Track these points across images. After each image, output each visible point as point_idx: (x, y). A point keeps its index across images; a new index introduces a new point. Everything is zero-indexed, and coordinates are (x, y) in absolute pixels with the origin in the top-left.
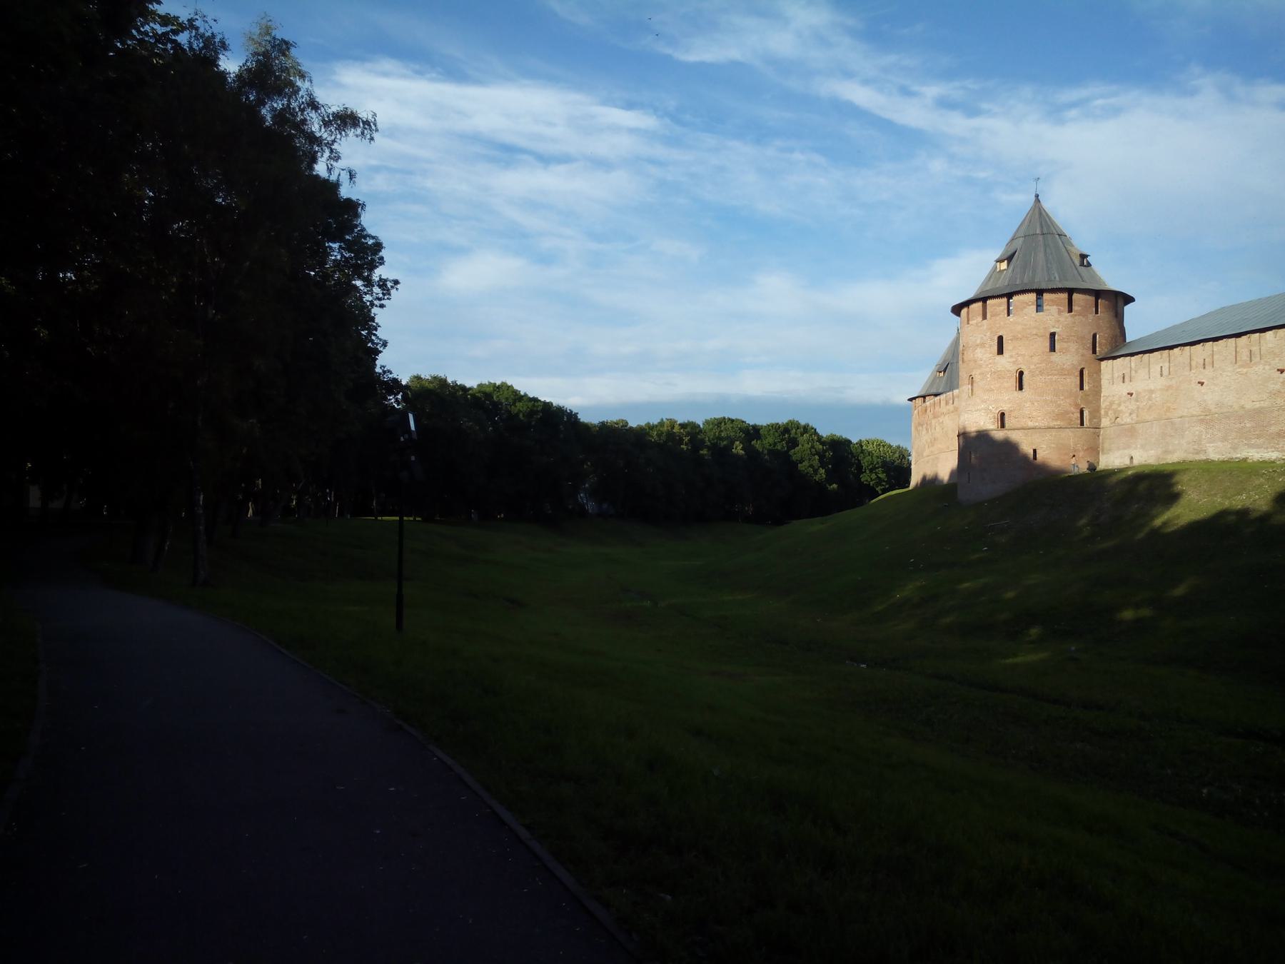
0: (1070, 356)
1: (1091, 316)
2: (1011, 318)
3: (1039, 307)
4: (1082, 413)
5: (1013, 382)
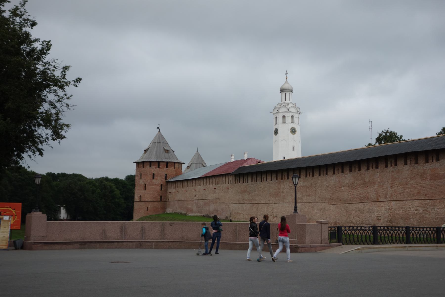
0: (159, 180)
1: (165, 169)
2: (144, 169)
3: (150, 167)
4: (161, 197)
5: (143, 188)
